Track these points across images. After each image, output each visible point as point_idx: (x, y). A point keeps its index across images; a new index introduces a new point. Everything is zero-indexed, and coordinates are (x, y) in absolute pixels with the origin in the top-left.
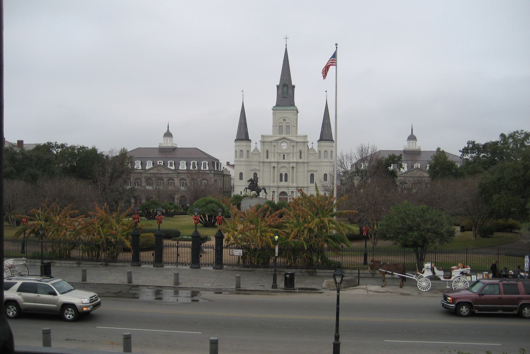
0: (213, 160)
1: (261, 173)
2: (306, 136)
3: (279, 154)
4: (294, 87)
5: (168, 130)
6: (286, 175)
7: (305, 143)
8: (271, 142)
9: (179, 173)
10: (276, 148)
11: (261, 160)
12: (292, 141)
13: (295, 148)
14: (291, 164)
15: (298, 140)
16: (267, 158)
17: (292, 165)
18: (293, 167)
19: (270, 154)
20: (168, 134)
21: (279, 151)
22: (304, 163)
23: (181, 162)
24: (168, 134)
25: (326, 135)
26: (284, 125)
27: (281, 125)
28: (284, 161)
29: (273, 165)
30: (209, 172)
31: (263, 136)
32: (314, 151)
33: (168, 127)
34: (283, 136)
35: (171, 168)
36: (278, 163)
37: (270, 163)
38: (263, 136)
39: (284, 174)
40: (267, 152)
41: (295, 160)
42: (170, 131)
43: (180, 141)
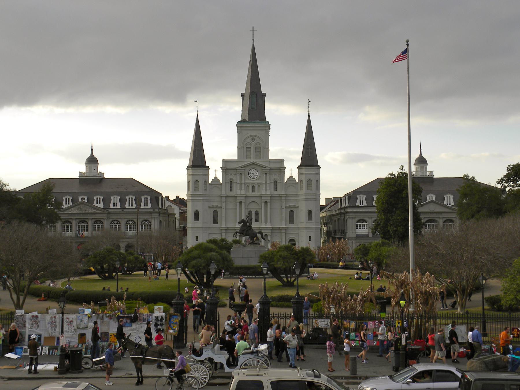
0: (157, 195)
1: (224, 211)
2: (282, 161)
3: (247, 185)
4: (264, 95)
5: (92, 154)
6: (257, 213)
8: (236, 169)
9: (109, 213)
10: (243, 177)
11: (224, 193)
13: (268, 177)
14: (263, 198)
15: (272, 166)
16: (231, 190)
17: (264, 199)
18: (266, 203)
19: (234, 185)
20: (92, 161)
21: (247, 181)
22: (280, 196)
23: (112, 198)
24: (92, 161)
25: (309, 159)
26: (253, 146)
28: (253, 194)
29: (239, 199)
30: (151, 210)
31: (224, 161)
32: (294, 180)
33: (92, 150)
34: (253, 160)
35: (98, 205)
36: (246, 197)
37: (236, 197)
38: (224, 161)
39: (253, 212)
40: (231, 182)
41: (268, 193)
42: (95, 155)
43: (109, 170)
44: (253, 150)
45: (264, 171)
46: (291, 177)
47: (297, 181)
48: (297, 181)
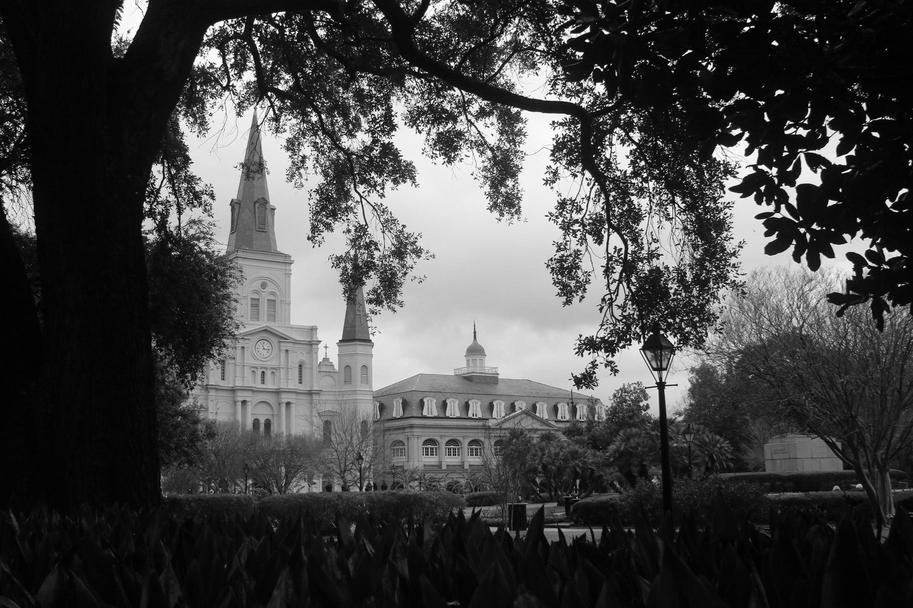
2: (313, 330)
3: (254, 369)
7: (312, 344)
12: (282, 338)
27: (256, 296)
32: (332, 365)
44: (264, 307)
45: (284, 346)
46: (326, 359)
47: (336, 367)
48: (336, 367)
